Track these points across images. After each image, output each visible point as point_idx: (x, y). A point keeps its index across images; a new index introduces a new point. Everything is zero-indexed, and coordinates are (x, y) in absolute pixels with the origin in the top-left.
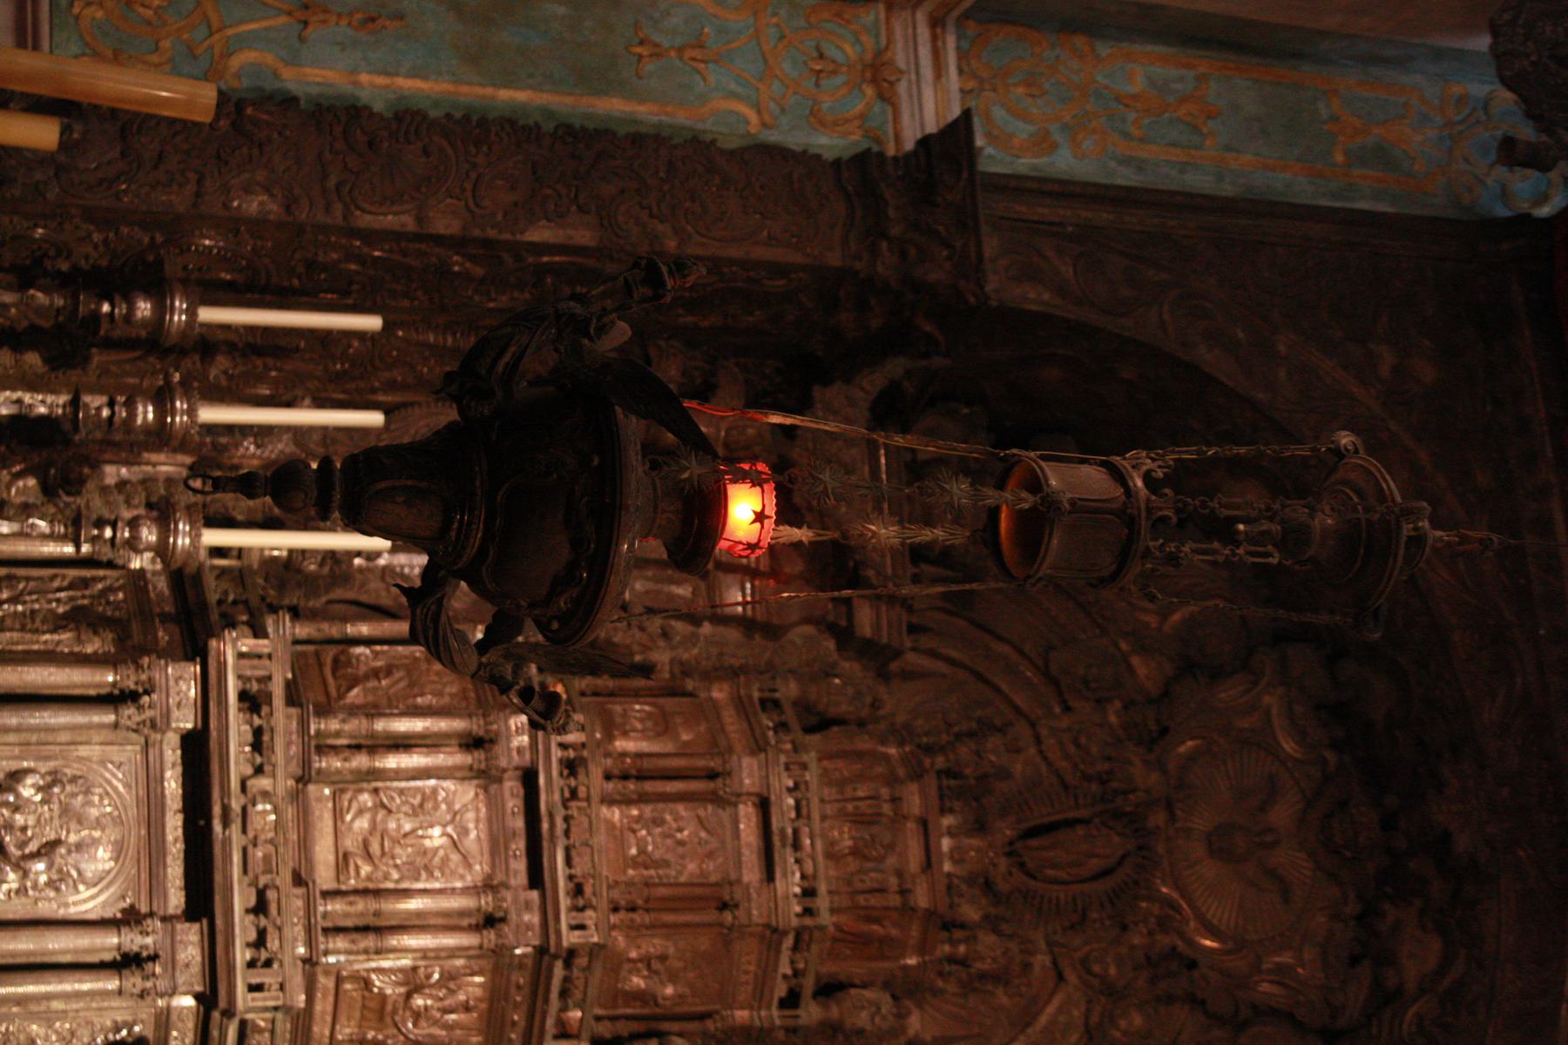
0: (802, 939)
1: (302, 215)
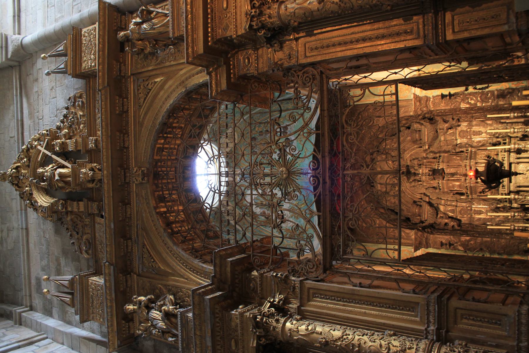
1: (497, 239)
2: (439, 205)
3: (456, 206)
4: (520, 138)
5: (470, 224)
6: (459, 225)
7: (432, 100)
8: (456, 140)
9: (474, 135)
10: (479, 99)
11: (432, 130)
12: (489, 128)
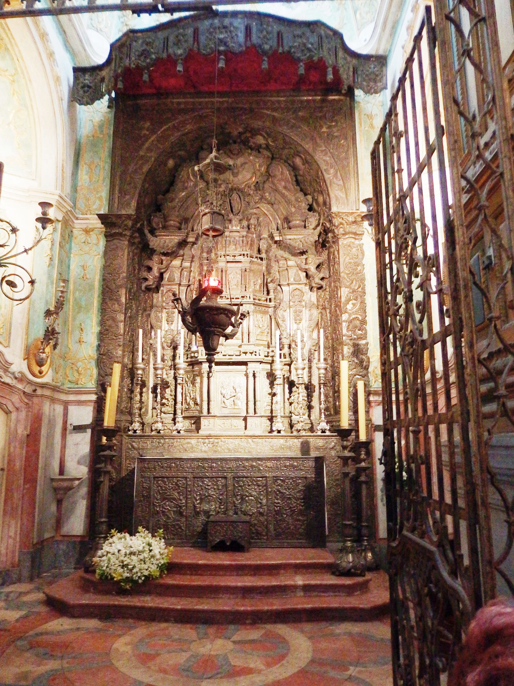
1: (121, 343)
2: (181, 258)
3: (180, 285)
4: (288, 378)
5: (152, 307)
6: (148, 289)
7: (357, 242)
8: (288, 284)
9: (295, 312)
10: (354, 316)
11: (305, 244)
12: (306, 335)
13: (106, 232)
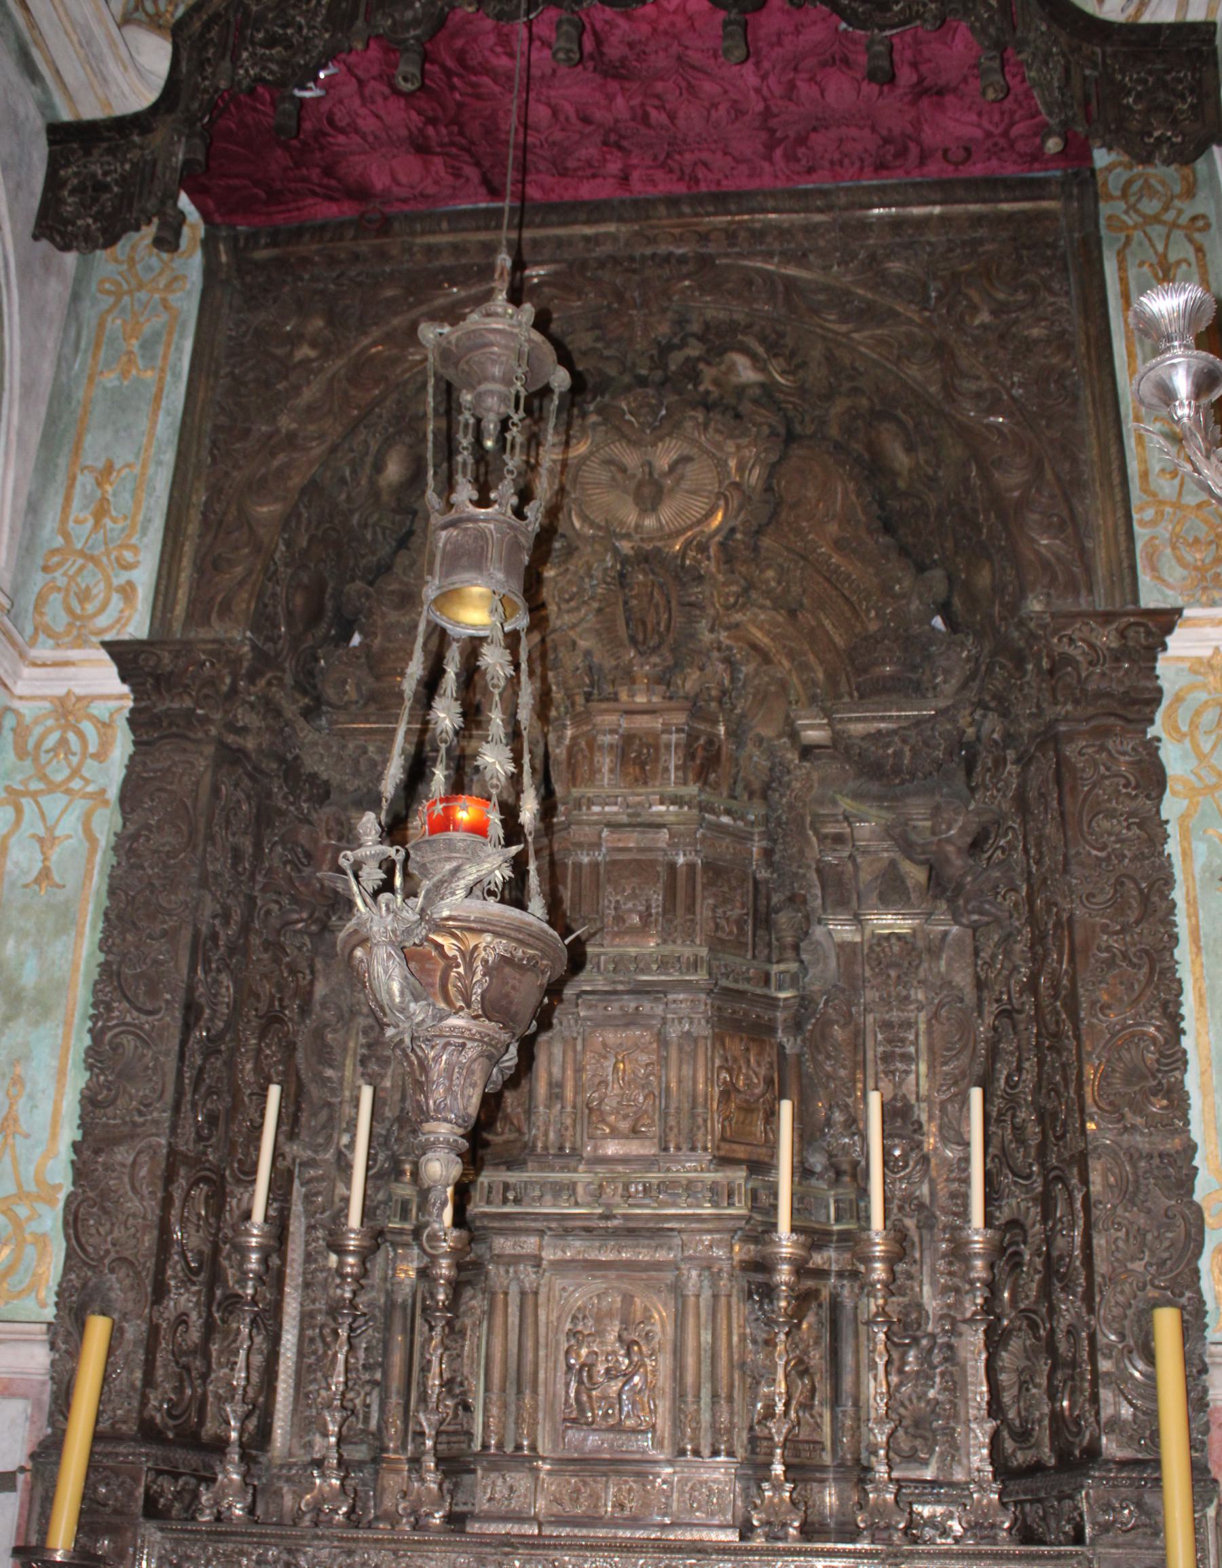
0: (704, 807)
13: (132, 711)
